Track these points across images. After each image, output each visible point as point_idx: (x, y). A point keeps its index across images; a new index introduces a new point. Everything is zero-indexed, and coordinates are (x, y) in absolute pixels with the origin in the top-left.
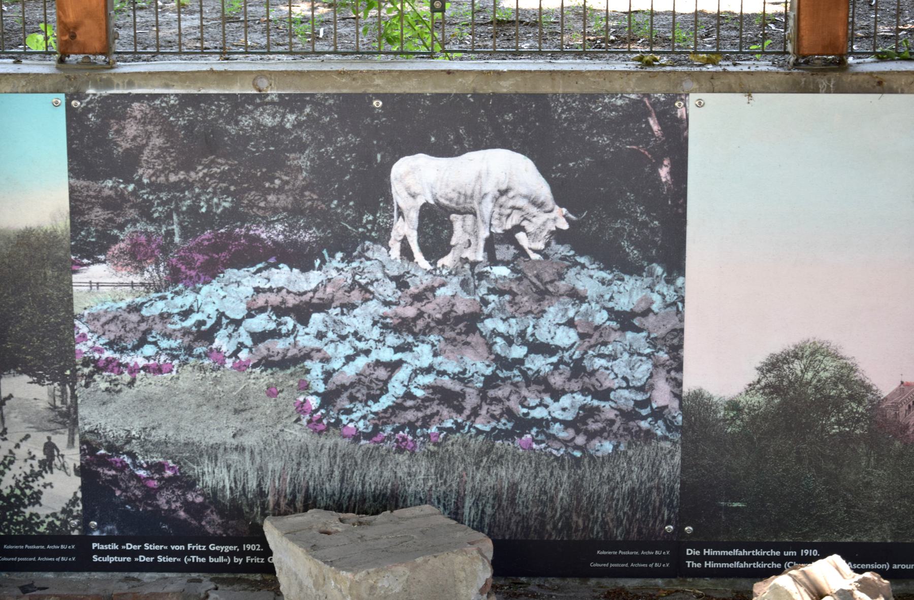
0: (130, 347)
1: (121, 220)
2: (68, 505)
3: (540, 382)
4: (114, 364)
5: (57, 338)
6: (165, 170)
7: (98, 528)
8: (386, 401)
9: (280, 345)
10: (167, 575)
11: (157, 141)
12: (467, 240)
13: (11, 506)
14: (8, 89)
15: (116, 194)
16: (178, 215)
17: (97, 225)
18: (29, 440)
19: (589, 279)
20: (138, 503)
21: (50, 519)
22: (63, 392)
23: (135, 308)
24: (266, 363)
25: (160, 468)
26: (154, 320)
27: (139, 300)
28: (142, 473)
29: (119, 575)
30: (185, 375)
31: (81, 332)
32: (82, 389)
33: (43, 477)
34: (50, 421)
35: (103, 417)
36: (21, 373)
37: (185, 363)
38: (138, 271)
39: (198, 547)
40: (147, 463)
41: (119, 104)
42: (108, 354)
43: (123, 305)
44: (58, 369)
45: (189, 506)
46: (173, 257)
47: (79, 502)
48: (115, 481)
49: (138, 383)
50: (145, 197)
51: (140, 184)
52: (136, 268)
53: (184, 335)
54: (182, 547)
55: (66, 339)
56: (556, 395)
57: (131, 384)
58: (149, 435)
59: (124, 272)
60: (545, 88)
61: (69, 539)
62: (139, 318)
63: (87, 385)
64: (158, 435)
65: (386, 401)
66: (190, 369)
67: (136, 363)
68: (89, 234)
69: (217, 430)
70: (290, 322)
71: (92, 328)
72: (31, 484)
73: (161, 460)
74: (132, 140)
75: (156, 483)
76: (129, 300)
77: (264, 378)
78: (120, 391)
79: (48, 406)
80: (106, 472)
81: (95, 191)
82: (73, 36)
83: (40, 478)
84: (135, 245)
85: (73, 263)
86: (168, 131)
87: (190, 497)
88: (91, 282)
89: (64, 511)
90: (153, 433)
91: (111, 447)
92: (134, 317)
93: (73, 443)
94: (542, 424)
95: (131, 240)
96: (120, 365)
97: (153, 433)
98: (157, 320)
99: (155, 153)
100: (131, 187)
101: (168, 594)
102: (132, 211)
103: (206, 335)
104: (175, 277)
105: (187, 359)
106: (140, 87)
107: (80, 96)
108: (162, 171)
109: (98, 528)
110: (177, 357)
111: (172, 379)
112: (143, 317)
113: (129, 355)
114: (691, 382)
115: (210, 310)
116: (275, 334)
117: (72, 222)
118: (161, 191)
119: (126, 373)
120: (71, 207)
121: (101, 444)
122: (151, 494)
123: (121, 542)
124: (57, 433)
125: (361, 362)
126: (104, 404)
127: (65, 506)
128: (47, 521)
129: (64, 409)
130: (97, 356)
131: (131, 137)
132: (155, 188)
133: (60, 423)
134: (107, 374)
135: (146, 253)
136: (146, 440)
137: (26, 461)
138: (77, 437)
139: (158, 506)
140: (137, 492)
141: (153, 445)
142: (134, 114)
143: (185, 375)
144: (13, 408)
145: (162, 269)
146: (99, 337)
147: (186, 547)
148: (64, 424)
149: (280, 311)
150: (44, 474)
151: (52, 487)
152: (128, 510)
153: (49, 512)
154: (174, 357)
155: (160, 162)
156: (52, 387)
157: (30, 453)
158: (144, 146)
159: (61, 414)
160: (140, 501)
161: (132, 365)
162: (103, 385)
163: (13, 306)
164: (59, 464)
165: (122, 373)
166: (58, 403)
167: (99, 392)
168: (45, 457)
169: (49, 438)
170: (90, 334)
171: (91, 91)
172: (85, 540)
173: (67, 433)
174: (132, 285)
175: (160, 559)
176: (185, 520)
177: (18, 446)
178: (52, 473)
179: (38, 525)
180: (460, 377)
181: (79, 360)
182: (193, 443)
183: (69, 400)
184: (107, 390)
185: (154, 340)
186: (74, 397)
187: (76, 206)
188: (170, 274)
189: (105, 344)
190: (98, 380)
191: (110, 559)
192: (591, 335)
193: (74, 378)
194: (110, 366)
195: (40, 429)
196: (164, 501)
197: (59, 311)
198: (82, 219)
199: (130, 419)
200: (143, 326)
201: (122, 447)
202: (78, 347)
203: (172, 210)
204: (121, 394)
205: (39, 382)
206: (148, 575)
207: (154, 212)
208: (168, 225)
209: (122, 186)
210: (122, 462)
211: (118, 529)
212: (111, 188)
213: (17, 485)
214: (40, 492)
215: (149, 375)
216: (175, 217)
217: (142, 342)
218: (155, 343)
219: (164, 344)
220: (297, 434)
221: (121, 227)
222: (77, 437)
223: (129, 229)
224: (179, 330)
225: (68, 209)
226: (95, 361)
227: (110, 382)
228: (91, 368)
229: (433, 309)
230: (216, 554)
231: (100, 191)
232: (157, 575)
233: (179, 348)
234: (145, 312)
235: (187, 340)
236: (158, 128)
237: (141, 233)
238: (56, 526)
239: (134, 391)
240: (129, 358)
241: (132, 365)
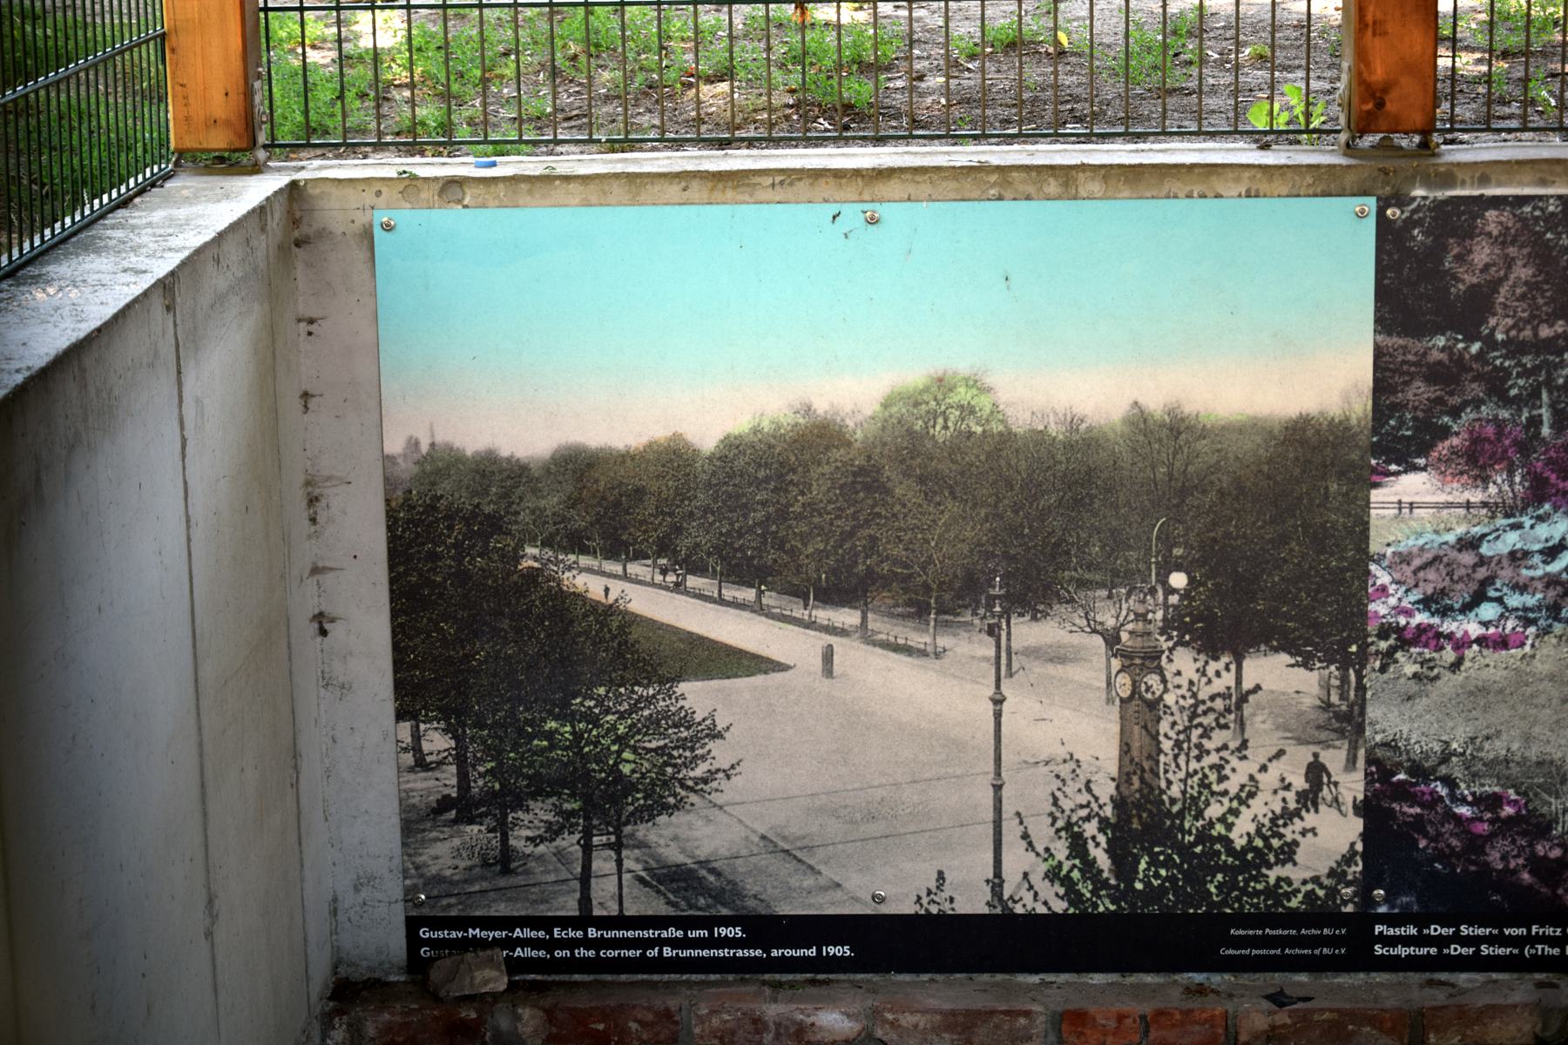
0: (1457, 606)
1: (1455, 400)
2: (1339, 864)
4: (1431, 634)
5: (1340, 593)
6: (1535, 319)
7: (1386, 900)
10: (1494, 976)
11: (1523, 272)
13: (1245, 866)
14: (1285, 191)
15: (1451, 359)
16: (1550, 392)
17: (1415, 408)
18: (1284, 758)
20: (1454, 860)
21: (1309, 887)
22: (1344, 680)
23: (1469, 544)
25: (1494, 801)
26: (1499, 562)
27: (1477, 530)
28: (1464, 811)
29: (1415, 978)
30: (1545, 651)
31: (1379, 582)
32: (1374, 676)
33: (1302, 819)
34: (1319, 727)
36: (1276, 650)
37: (1547, 631)
38: (1479, 482)
39: (1549, 931)
40: (1473, 794)
41: (1463, 213)
42: (1421, 618)
43: (1451, 538)
44: (1338, 643)
45: (1538, 865)
46: (1538, 460)
47: (1358, 858)
48: (1418, 824)
49: (1467, 664)
50: (1498, 362)
51: (1490, 343)
52: (1476, 478)
53: (1547, 586)
54: (1522, 931)
55: (1354, 595)
57: (1456, 666)
58: (1481, 749)
59: (1455, 485)
61: (1337, 919)
62: (1477, 560)
63: (1383, 669)
64: (1495, 749)
66: (1554, 641)
67: (1466, 633)
68: (1402, 423)
71: (1397, 576)
72: (1282, 830)
73: (1497, 789)
74: (1482, 271)
75: (1486, 826)
76: (1460, 530)
78: (1437, 677)
79: (1318, 703)
80: (1406, 809)
81: (1416, 354)
82: (1380, 104)
83: (1296, 820)
84: (1476, 440)
85: (1374, 470)
86: (1543, 256)
87: (1539, 850)
88: (1400, 502)
89: (1332, 873)
90: (1487, 746)
91: (1419, 771)
92: (1468, 558)
93: (1354, 763)
95: (1471, 433)
96: (1439, 635)
97: (1487, 746)
98: (1505, 563)
99: (1519, 291)
100: (1475, 347)
101: (1515, 1006)
102: (1474, 385)
104: (1538, 494)
105: (1550, 626)
106: (1499, 184)
107: (1400, 200)
108: (1528, 321)
109: (1386, 900)
110: (1533, 622)
111: (1524, 656)
112: (1481, 557)
113: (1454, 620)
117: (1375, 404)
118: (1524, 353)
119: (1449, 648)
120: (1375, 380)
121: (1400, 764)
122: (1475, 845)
123: (1422, 923)
124: (1329, 747)
126: (1409, 698)
127: (1334, 865)
128: (1304, 889)
129: (1344, 708)
130: (1402, 621)
131: (1480, 266)
132: (1515, 348)
133: (1335, 730)
134: (1418, 650)
135: (1495, 453)
136: (1474, 757)
137: (1275, 792)
138: (1362, 753)
139: (1487, 864)
140: (1454, 842)
141: (1485, 765)
142: (1488, 229)
143: (1545, 651)
144: (1260, 707)
145: (1517, 479)
146: (1407, 591)
147: (1529, 931)
148: (1341, 733)
150: (1303, 813)
151: (1315, 834)
152: (1438, 871)
153: (1308, 875)
154: (1528, 622)
155: (1525, 306)
156: (1327, 672)
157: (1283, 780)
158: (1500, 281)
159: (1339, 716)
160: (1458, 856)
161: (1459, 635)
162: (1410, 669)
163: (1272, 541)
164: (1329, 798)
165: (1442, 648)
166: (1335, 699)
167: (1402, 680)
168: (1307, 786)
169: (1316, 755)
170: (1394, 586)
171: (1419, 192)
172: (1364, 919)
173: (1346, 746)
174: (1468, 505)
175: (1485, 950)
176: (1530, 887)
177: (1264, 768)
178: (1317, 811)
179: (1288, 896)
181: (1372, 628)
182: (1552, 762)
183: (1352, 693)
184: (1415, 676)
185: (1498, 594)
186: (1361, 688)
187: (1383, 379)
188: (1531, 487)
189: (1418, 602)
190: (1402, 660)
191: (1402, 951)
193: (1363, 658)
194: (1424, 638)
195: (1301, 741)
196: (1498, 855)
197: (1345, 550)
198: (1392, 399)
199: (1451, 724)
200: (1482, 573)
201: (1434, 769)
202: (1372, 607)
203: (1540, 385)
204: (1438, 683)
205: (1306, 664)
206: (1464, 976)
207: (1511, 387)
208: (1534, 407)
209: (1461, 345)
210: (1433, 792)
211: (1419, 901)
212: (1443, 350)
213: (1259, 832)
214: (1295, 843)
215: (1485, 652)
216: (1545, 396)
217: (1479, 598)
218: (1500, 600)
219: (1514, 600)
221: (1455, 413)
222: (1362, 753)
223: (1468, 415)
224: (1540, 578)
225: (1371, 383)
226: (1400, 630)
227: (1422, 664)
228: (1391, 641)
230: (1533, 940)
231: (1425, 354)
232: (1479, 977)
233: (1539, 608)
234: (1485, 549)
235: (1552, 593)
236: (1525, 251)
237: (1488, 421)
238: (1318, 898)
239: (1459, 678)
240: (1455, 624)
241: (1459, 635)
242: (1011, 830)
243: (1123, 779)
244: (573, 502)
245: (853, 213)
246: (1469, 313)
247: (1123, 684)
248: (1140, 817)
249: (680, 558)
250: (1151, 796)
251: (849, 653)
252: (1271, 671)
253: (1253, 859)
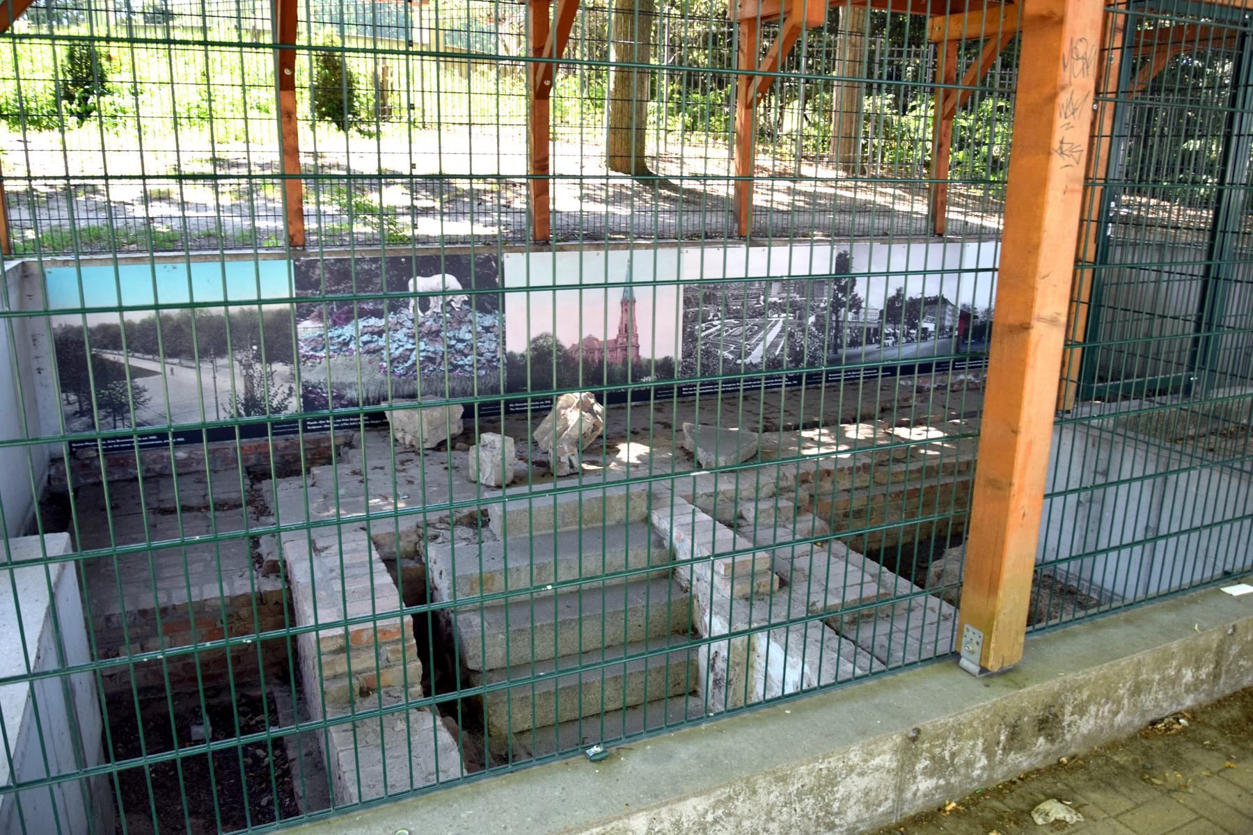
3: (461, 352)
8: (410, 362)
9: (373, 345)
11: (327, 276)
12: (435, 304)
19: (477, 317)
23: (320, 336)
24: (368, 352)
35: (310, 376)
56: (466, 356)
60: (458, 253)
65: (410, 362)
69: (351, 377)
70: (376, 337)
77: (367, 357)
86: (331, 272)
91: (314, 387)
94: (462, 366)
103: (346, 344)
104: (335, 323)
114: (508, 350)
115: (348, 335)
116: (371, 342)
125: (401, 349)
149: (372, 333)
180: (434, 352)
192: (478, 336)
220: (379, 376)
229: (424, 329)
242: (220, 408)
243: (246, 394)
244: (104, 337)
245: (169, 266)
246: (316, 285)
247: (244, 372)
248: (252, 404)
249: (133, 349)
250: (253, 397)
251: (177, 369)
252: (278, 367)
253: (277, 410)
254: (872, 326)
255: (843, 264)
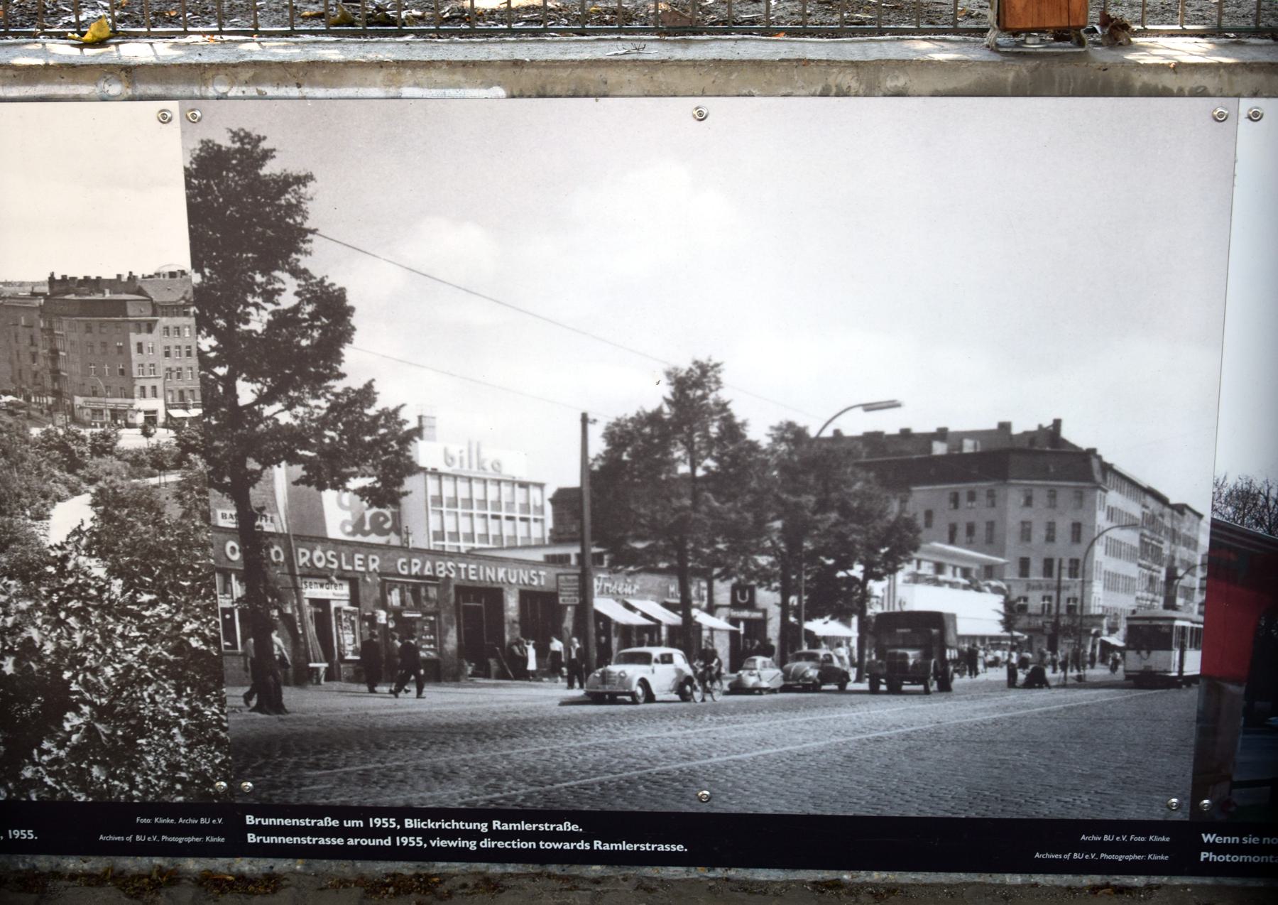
254: (513, 580)
255: (243, 212)
